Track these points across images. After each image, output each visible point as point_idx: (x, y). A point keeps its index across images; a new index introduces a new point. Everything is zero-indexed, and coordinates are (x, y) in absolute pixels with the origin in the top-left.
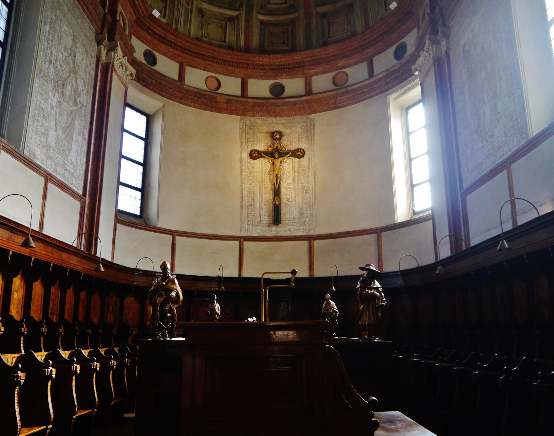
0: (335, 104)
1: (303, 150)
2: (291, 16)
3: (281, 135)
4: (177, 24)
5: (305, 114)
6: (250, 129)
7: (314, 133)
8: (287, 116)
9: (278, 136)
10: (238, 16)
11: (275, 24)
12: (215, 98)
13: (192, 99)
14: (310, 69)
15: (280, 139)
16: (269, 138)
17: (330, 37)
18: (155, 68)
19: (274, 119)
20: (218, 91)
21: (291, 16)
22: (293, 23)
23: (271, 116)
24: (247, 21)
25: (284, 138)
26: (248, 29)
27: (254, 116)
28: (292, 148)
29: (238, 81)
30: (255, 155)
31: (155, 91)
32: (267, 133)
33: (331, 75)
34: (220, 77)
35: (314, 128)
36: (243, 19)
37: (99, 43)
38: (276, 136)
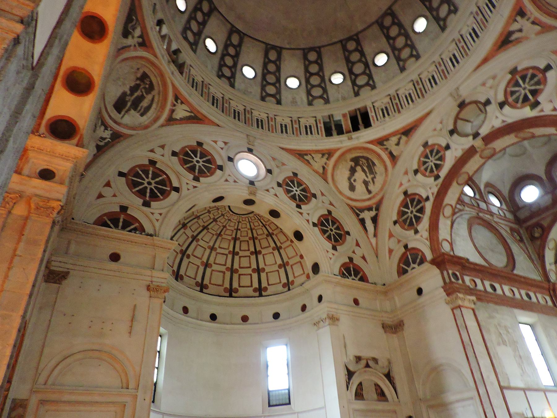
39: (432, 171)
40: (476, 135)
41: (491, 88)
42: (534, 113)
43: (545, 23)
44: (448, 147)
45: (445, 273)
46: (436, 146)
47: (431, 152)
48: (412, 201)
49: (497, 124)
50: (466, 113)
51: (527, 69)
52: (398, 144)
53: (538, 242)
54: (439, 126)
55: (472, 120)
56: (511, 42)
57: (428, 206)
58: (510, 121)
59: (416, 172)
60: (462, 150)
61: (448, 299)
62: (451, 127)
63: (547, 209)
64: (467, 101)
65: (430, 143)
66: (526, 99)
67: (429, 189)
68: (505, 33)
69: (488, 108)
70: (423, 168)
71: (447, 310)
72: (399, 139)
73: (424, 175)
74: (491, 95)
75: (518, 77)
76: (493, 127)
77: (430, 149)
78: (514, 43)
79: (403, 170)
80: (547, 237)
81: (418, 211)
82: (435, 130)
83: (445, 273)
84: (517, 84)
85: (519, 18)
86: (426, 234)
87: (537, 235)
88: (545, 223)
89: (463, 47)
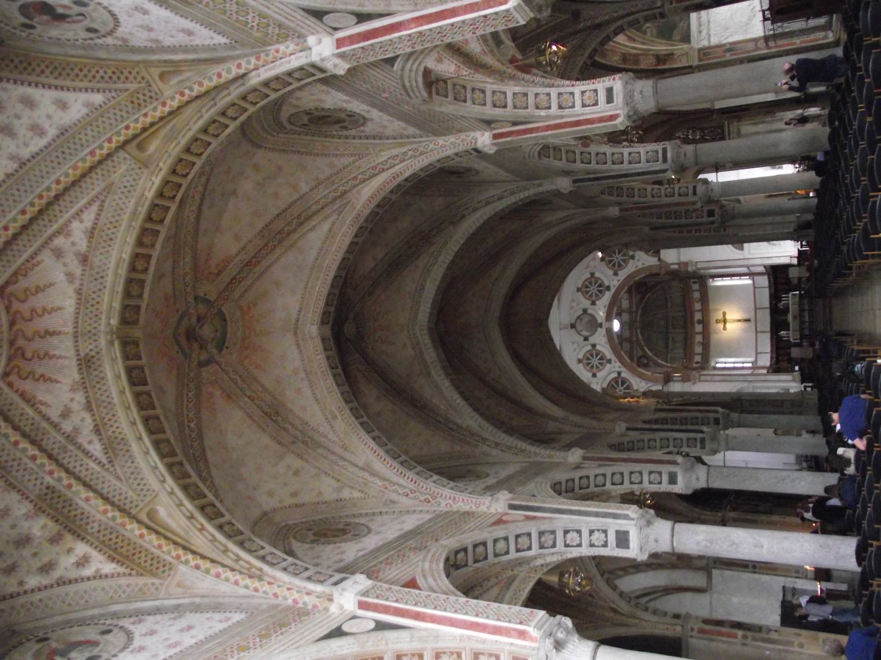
39: (601, 364)
40: (601, 325)
42: (613, 290)
44: (594, 346)
47: (588, 359)
53: (651, 364)
54: (575, 346)
57: (626, 374)
58: (607, 303)
62: (582, 338)
63: (632, 348)
64: (573, 322)
65: (581, 357)
66: (600, 291)
69: (589, 311)
73: (601, 370)
74: (582, 306)
81: (622, 385)
82: (575, 350)
84: (587, 292)
87: (645, 361)
88: (640, 353)
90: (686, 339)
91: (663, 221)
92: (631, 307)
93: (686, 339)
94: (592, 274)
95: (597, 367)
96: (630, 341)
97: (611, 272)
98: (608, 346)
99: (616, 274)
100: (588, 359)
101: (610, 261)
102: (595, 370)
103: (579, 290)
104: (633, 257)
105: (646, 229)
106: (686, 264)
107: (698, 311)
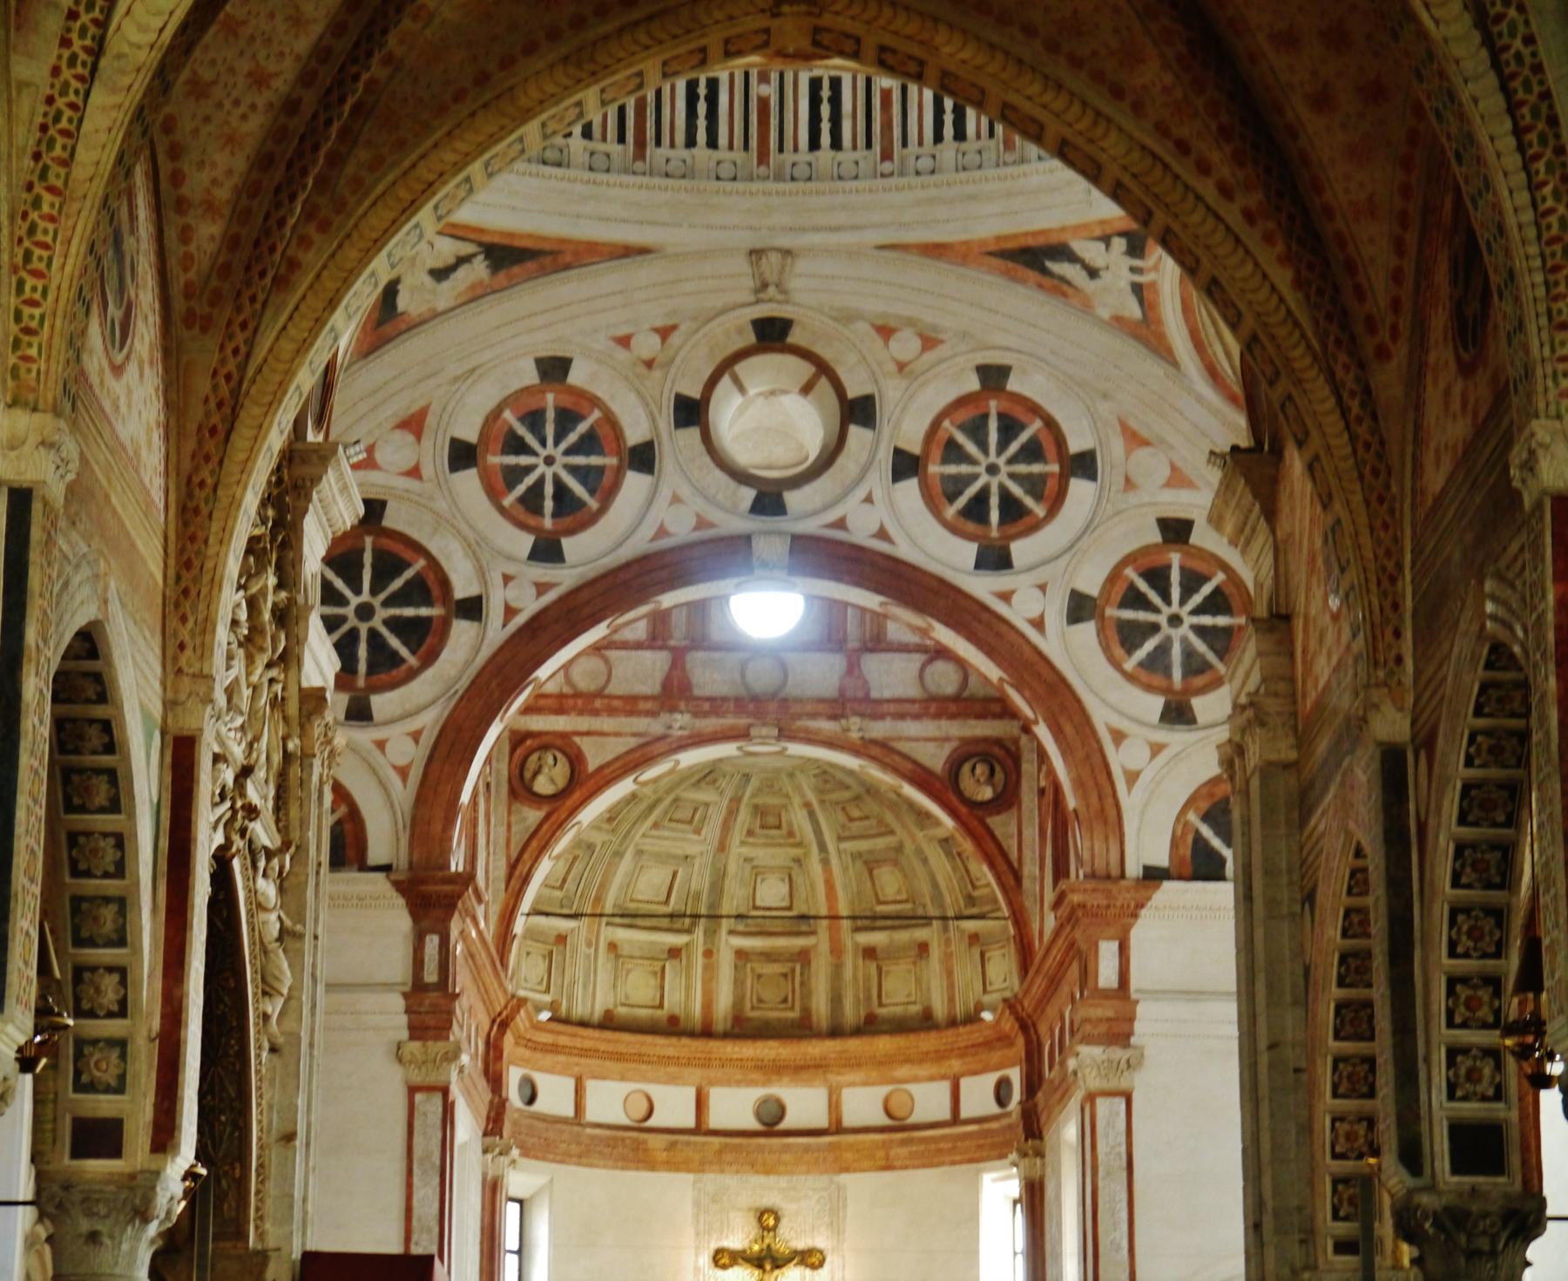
0: (887, 1158)
1: (821, 1252)
2: (800, 942)
3: (777, 1219)
4: (570, 998)
5: (826, 1172)
6: (714, 1201)
7: (845, 1217)
8: (791, 1173)
9: (771, 1222)
10: (687, 945)
11: (768, 956)
12: (645, 1142)
13: (600, 1153)
14: (839, 1074)
15: (775, 1228)
16: (754, 1222)
17: (881, 1005)
18: (538, 1106)
19: (762, 1179)
20: (651, 1123)
21: (800, 942)
22: (804, 957)
23: (757, 1172)
24: (708, 954)
25: (784, 1223)
26: (710, 970)
27: (722, 1171)
28: (800, 1245)
29: (690, 1093)
30: (724, 1258)
31: (536, 1158)
32: (750, 1209)
33: (883, 1090)
34: (655, 1090)
35: (845, 1206)
36: (700, 950)
37: (485, 1151)
38: (767, 1219)
39: (532, 501)
40: (769, 500)
41: (901, 366)
42: (982, 587)
43: (1159, 322)
44: (644, 458)
45: (432, 942)
46: (596, 414)
48: (387, 567)
49: (861, 532)
50: (764, 371)
51: (1035, 410)
52: (440, 274)
53: (533, 816)
54: (647, 344)
55: (752, 392)
56: (1045, 272)
58: (904, 550)
59: (462, 455)
60: (701, 523)
61: (415, 1046)
62: (695, 392)
63: (630, 705)
64: (794, 338)
65: (576, 377)
67: (499, 581)
68: (1054, 239)
69: (854, 431)
70: (496, 460)
71: (390, 1083)
72: (462, 260)
73: (494, 495)
74: (890, 395)
75: (993, 406)
76: (840, 524)
77: (567, 401)
78: (1047, 281)
79: (403, 405)
80: (574, 811)
82: (624, 341)
83: (432, 942)
84: (976, 430)
85: (1119, 244)
86: (406, 751)
87: (543, 786)
88: (595, 755)
89: (886, 95)
90: (673, 1027)
91: (1446, 832)
92: (873, 708)
93: (673, 1027)
94: (1084, 465)
95: (514, 475)
96: (675, 692)
97: (1091, 585)
98: (639, 544)
99: (1080, 608)
100: (567, 420)
101: (1157, 577)
102: (496, 460)
103: (993, 376)
104: (1178, 714)
105: (1392, 725)
106: (1119, 1033)
107: (834, 1106)
